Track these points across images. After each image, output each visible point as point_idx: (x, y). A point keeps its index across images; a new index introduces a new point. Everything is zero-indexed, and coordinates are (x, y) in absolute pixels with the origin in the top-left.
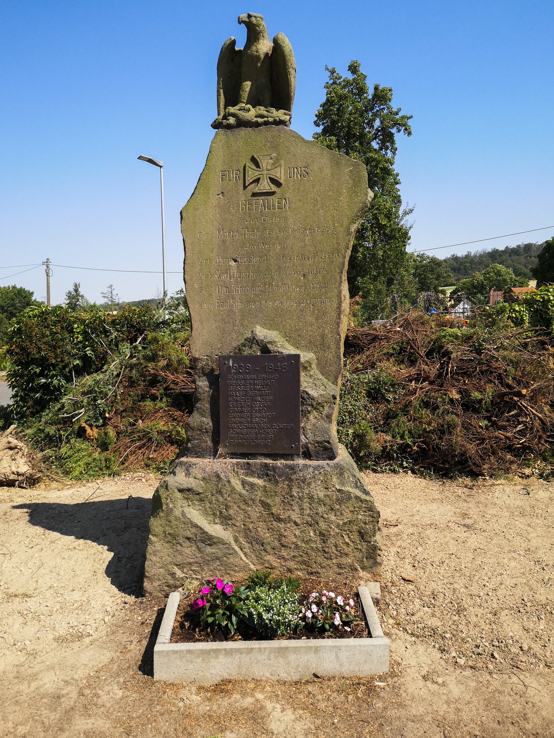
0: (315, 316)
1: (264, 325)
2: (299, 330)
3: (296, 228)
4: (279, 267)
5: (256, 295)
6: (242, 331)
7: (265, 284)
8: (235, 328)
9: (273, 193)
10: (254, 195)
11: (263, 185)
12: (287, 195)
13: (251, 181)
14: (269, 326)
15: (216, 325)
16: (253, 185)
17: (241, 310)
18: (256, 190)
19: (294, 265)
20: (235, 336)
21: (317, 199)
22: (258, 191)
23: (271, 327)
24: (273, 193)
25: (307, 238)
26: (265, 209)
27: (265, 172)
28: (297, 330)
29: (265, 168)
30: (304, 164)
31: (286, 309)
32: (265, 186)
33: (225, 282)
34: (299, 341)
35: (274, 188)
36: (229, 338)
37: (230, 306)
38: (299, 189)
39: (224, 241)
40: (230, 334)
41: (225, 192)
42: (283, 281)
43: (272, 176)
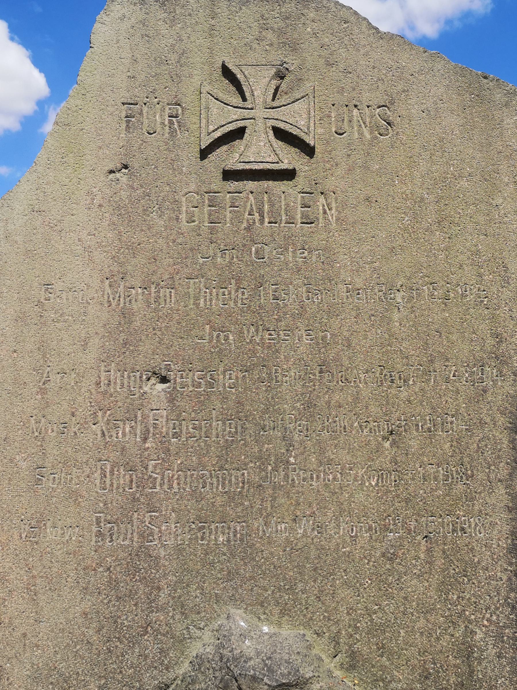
0: (435, 579)
1: (259, 606)
2: (382, 628)
3: (359, 282)
4: (309, 405)
5: (231, 497)
6: (179, 628)
7: (262, 459)
8: (154, 616)
9: (289, 175)
10: (229, 175)
11: (253, 149)
12: (330, 184)
13: (218, 134)
14: (276, 611)
15: (86, 605)
16: (224, 148)
17: (179, 550)
18: (234, 163)
19: (357, 399)
20: (152, 649)
21: (422, 199)
22: (240, 167)
23: (282, 614)
24: (289, 175)
25: (396, 316)
26: (262, 221)
27: (260, 113)
28: (374, 630)
29: (259, 101)
30: (380, 98)
31: (337, 549)
32: (260, 150)
33: (123, 449)
34: (383, 668)
35: (288, 157)
36: (132, 658)
37: (141, 536)
38: (366, 167)
39: (126, 315)
40: (133, 643)
41: (135, 164)
42: (322, 451)
43: (281, 125)
